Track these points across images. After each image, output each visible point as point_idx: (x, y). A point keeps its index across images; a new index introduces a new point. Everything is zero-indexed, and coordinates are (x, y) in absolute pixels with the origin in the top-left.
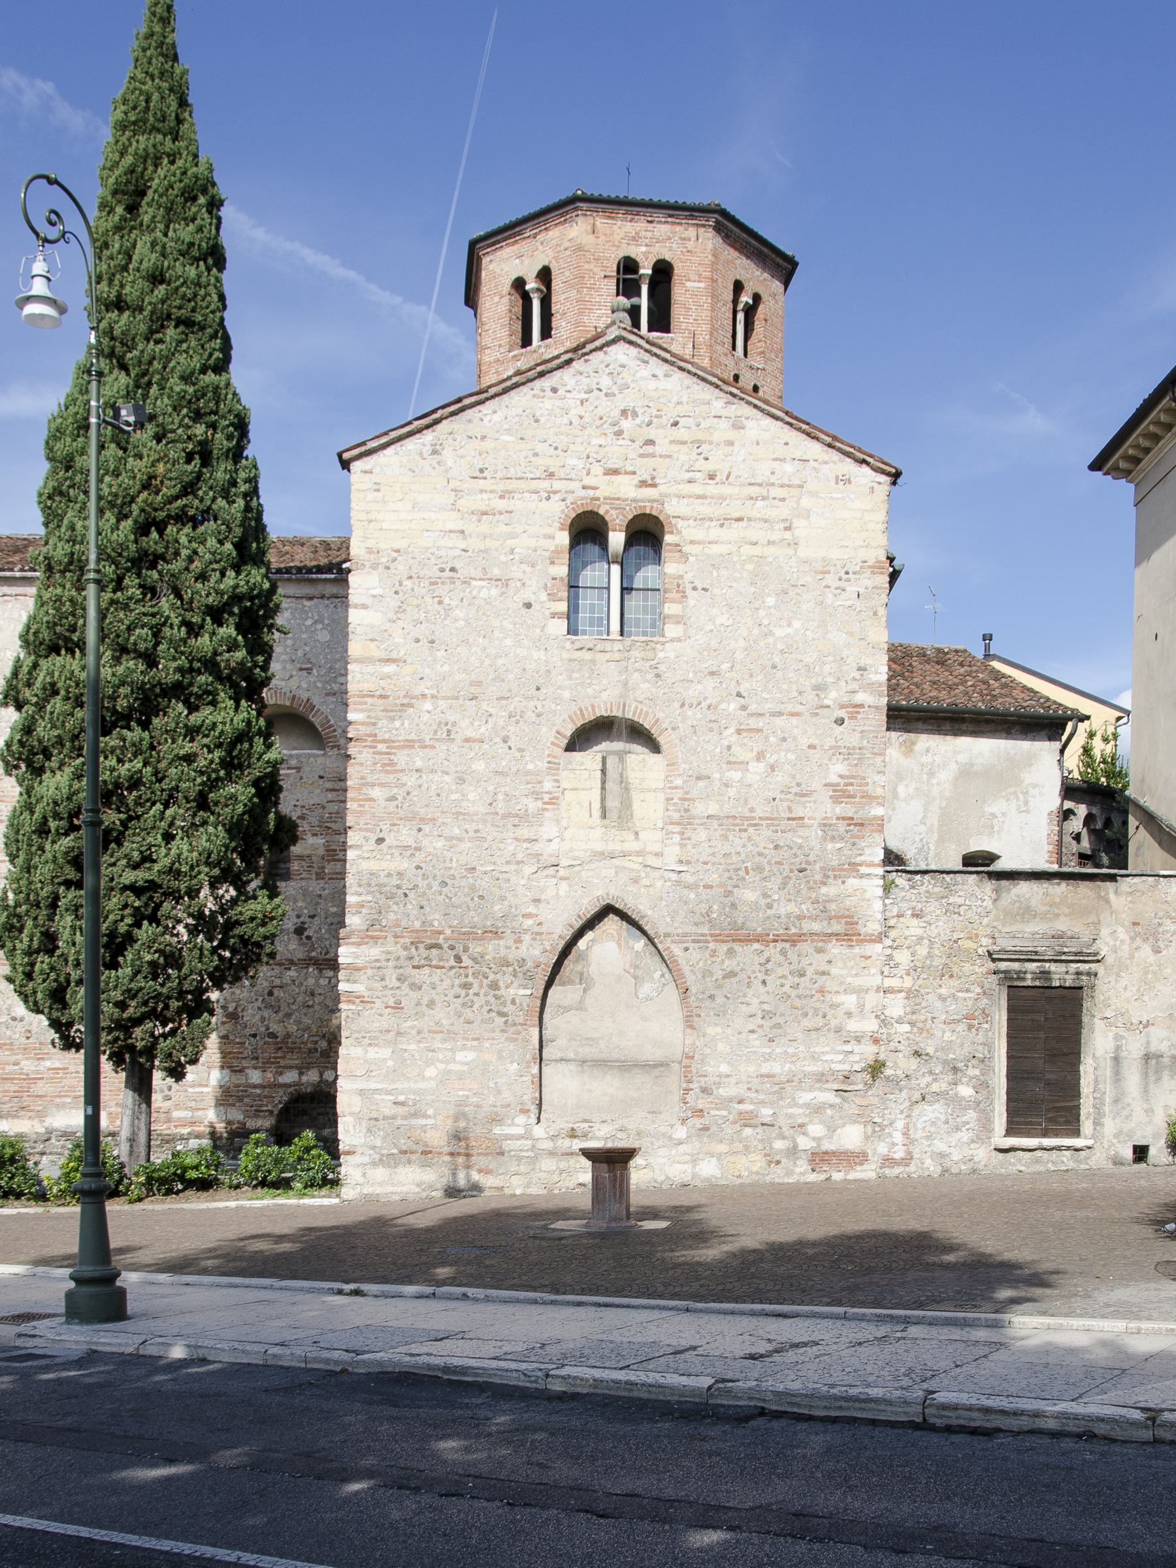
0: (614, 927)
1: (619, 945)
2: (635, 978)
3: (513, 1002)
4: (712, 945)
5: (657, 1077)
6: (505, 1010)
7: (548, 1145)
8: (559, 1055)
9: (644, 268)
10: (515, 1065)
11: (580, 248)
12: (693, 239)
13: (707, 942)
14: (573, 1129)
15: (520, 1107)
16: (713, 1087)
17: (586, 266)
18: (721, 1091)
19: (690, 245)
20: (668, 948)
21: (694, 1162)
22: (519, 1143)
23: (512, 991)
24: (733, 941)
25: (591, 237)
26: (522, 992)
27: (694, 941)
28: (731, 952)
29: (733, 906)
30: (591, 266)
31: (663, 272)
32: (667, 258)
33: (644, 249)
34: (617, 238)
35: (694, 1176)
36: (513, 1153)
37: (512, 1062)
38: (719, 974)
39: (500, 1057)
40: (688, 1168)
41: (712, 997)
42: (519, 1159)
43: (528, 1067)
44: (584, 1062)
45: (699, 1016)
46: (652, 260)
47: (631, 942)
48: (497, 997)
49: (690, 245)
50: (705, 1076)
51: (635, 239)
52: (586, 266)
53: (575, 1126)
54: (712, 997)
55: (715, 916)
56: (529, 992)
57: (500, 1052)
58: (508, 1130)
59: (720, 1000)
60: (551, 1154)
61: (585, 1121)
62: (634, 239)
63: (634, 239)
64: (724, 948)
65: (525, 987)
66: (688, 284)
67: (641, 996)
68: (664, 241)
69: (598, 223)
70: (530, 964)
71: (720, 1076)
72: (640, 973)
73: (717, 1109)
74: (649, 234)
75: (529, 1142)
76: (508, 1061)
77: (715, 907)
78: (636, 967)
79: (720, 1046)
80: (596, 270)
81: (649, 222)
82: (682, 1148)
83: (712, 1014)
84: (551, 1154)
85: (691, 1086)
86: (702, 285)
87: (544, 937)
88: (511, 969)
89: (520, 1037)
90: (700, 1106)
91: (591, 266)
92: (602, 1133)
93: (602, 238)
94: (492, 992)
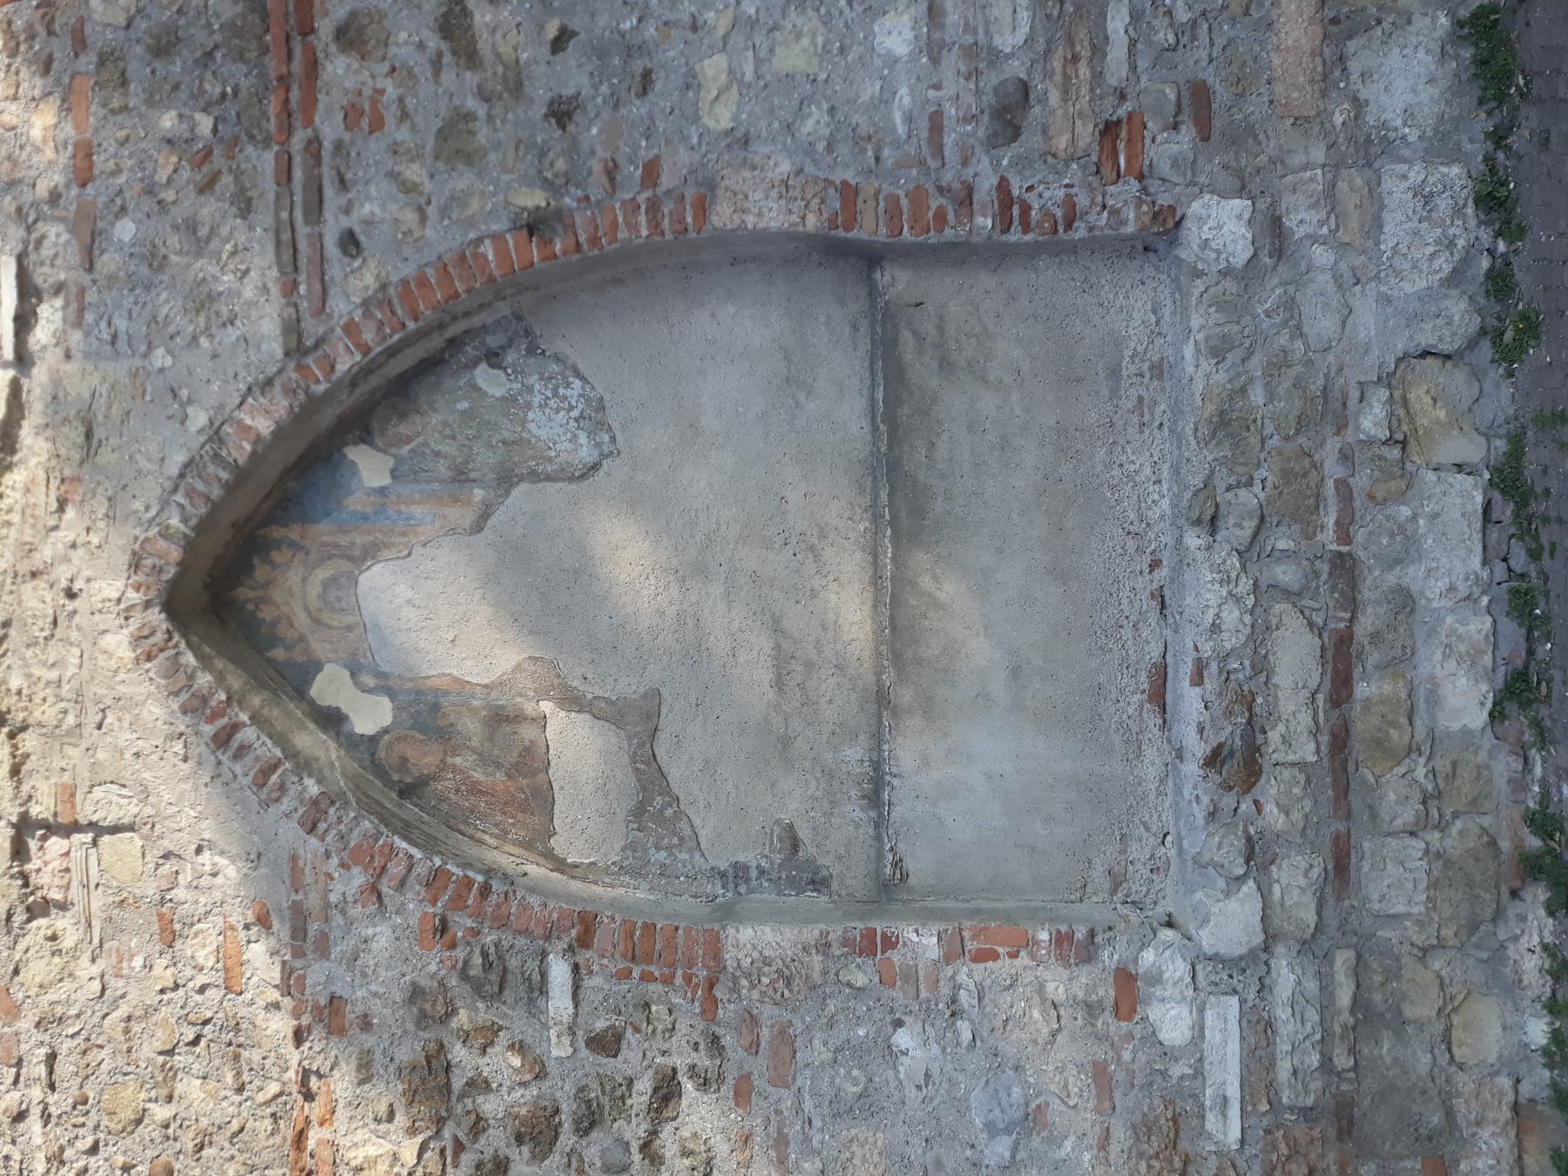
0: (294, 577)
1: (370, 553)
2: (506, 480)
3: (607, 1044)
4: (330, 128)
5: (946, 365)
6: (644, 1085)
7: (1295, 879)
8: (855, 810)
10: (902, 1039)
13: (314, 147)
14: (1214, 759)
15: (1106, 1020)
16: (991, 79)
18: (1008, 40)
20: (350, 328)
21: (1368, 149)
22: (1287, 1025)
23: (559, 1049)
24: (308, 30)
26: (559, 1002)
27: (315, 208)
28: (350, 36)
29: (163, 48)
35: (1440, 147)
36: (1342, 1061)
37: (891, 1054)
38: (460, 86)
39: (865, 1106)
40: (1399, 184)
41: (562, 113)
42: (1369, 1017)
43: (911, 976)
44: (882, 698)
45: (651, 171)
47: (356, 502)
48: (589, 1121)
50: (936, 124)
53: (1198, 749)
54: (562, 113)
55: (205, 123)
56: (559, 971)
57: (841, 1111)
58: (1226, 1075)
59: (573, 75)
60: (1341, 869)
61: (1158, 694)
64: (339, 69)
65: (540, 988)
67: (586, 453)
70: (432, 964)
71: (934, 50)
72: (485, 459)
73: (1099, 50)
75: (1286, 976)
76: (883, 1075)
77: (168, 121)
78: (462, 476)
79: (793, 57)
82: (1302, 219)
83: (636, 109)
84: (1341, 869)
85: (986, 185)
87: (313, 901)
88: (458, 1053)
89: (767, 1012)
90: (1086, 133)
92: (1231, 616)
94: (567, 1139)
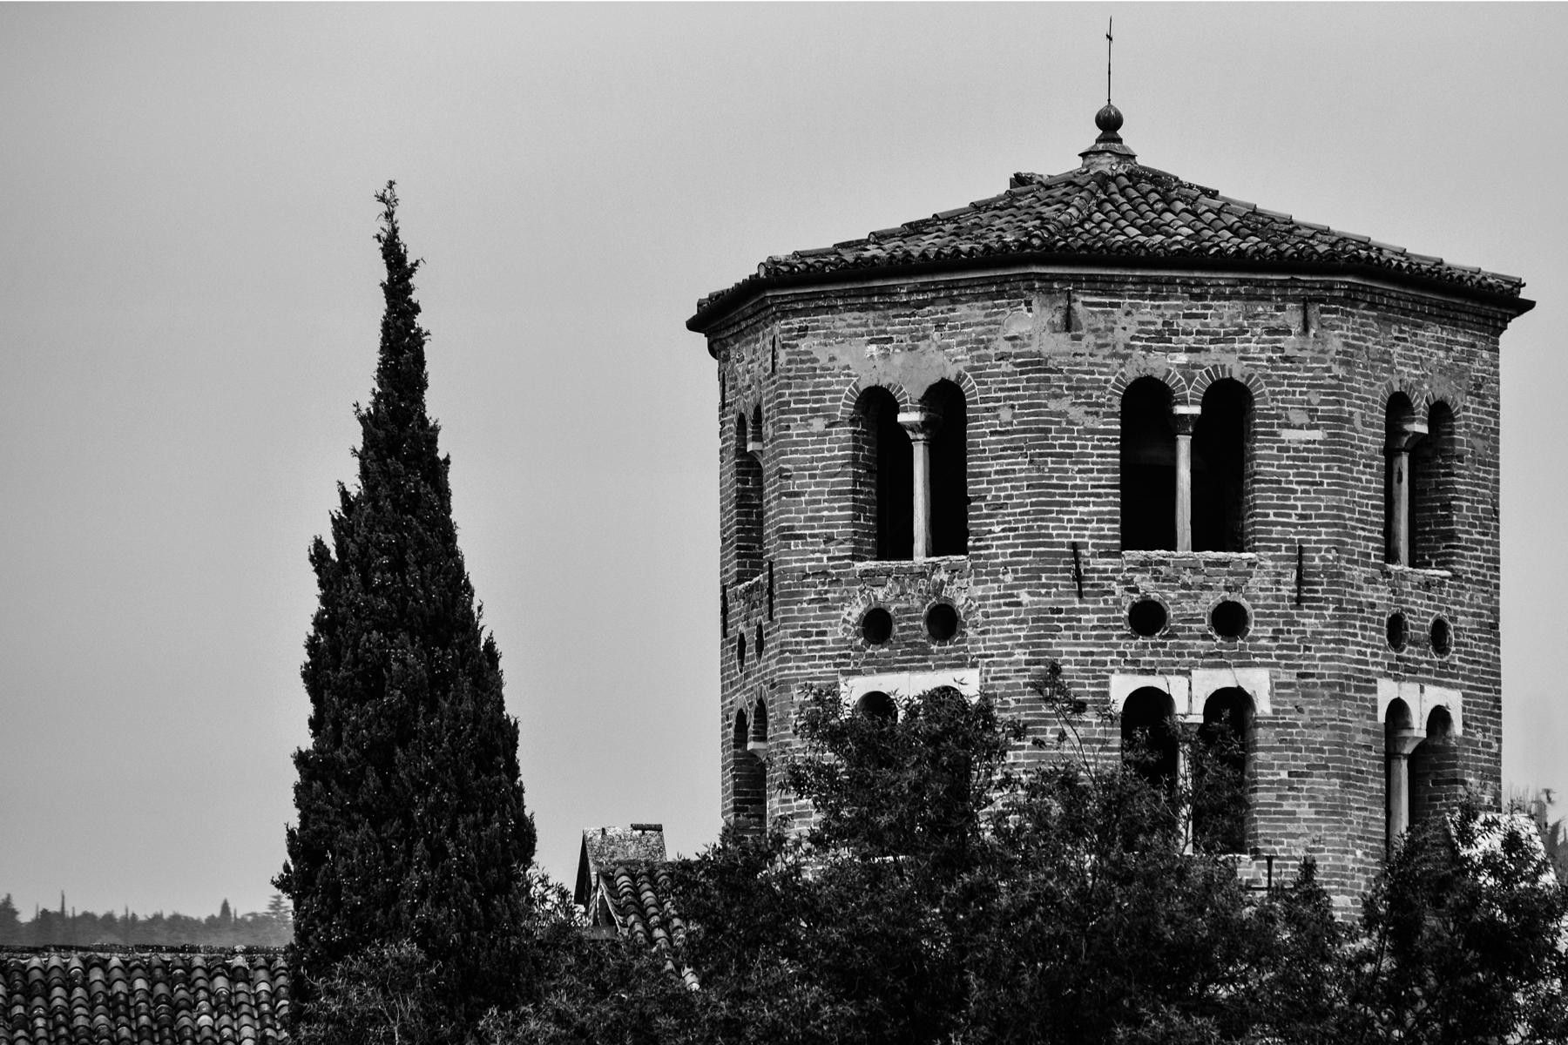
9: (1184, 402)
11: (1037, 365)
12: (1296, 329)
17: (1053, 405)
19: (1290, 343)
25: (1063, 338)
30: (1063, 405)
31: (1229, 405)
32: (1236, 376)
33: (1182, 358)
34: (1121, 337)
46: (1202, 382)
49: (1290, 343)
51: (1163, 337)
52: (1053, 405)
62: (1160, 337)
63: (1160, 337)
66: (1287, 434)
68: (1228, 338)
69: (1078, 306)
74: (1196, 325)
80: (1076, 413)
81: (1193, 297)
86: (1318, 435)
91: (1063, 405)
93: (1090, 339)
